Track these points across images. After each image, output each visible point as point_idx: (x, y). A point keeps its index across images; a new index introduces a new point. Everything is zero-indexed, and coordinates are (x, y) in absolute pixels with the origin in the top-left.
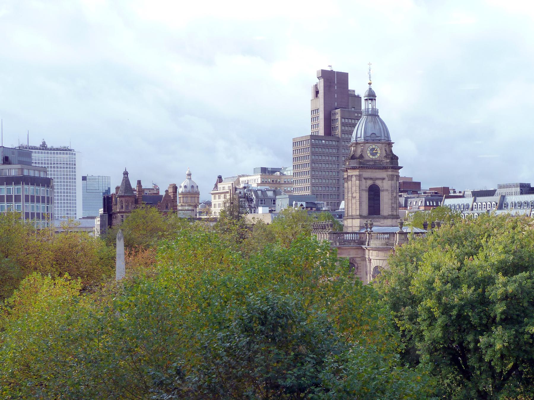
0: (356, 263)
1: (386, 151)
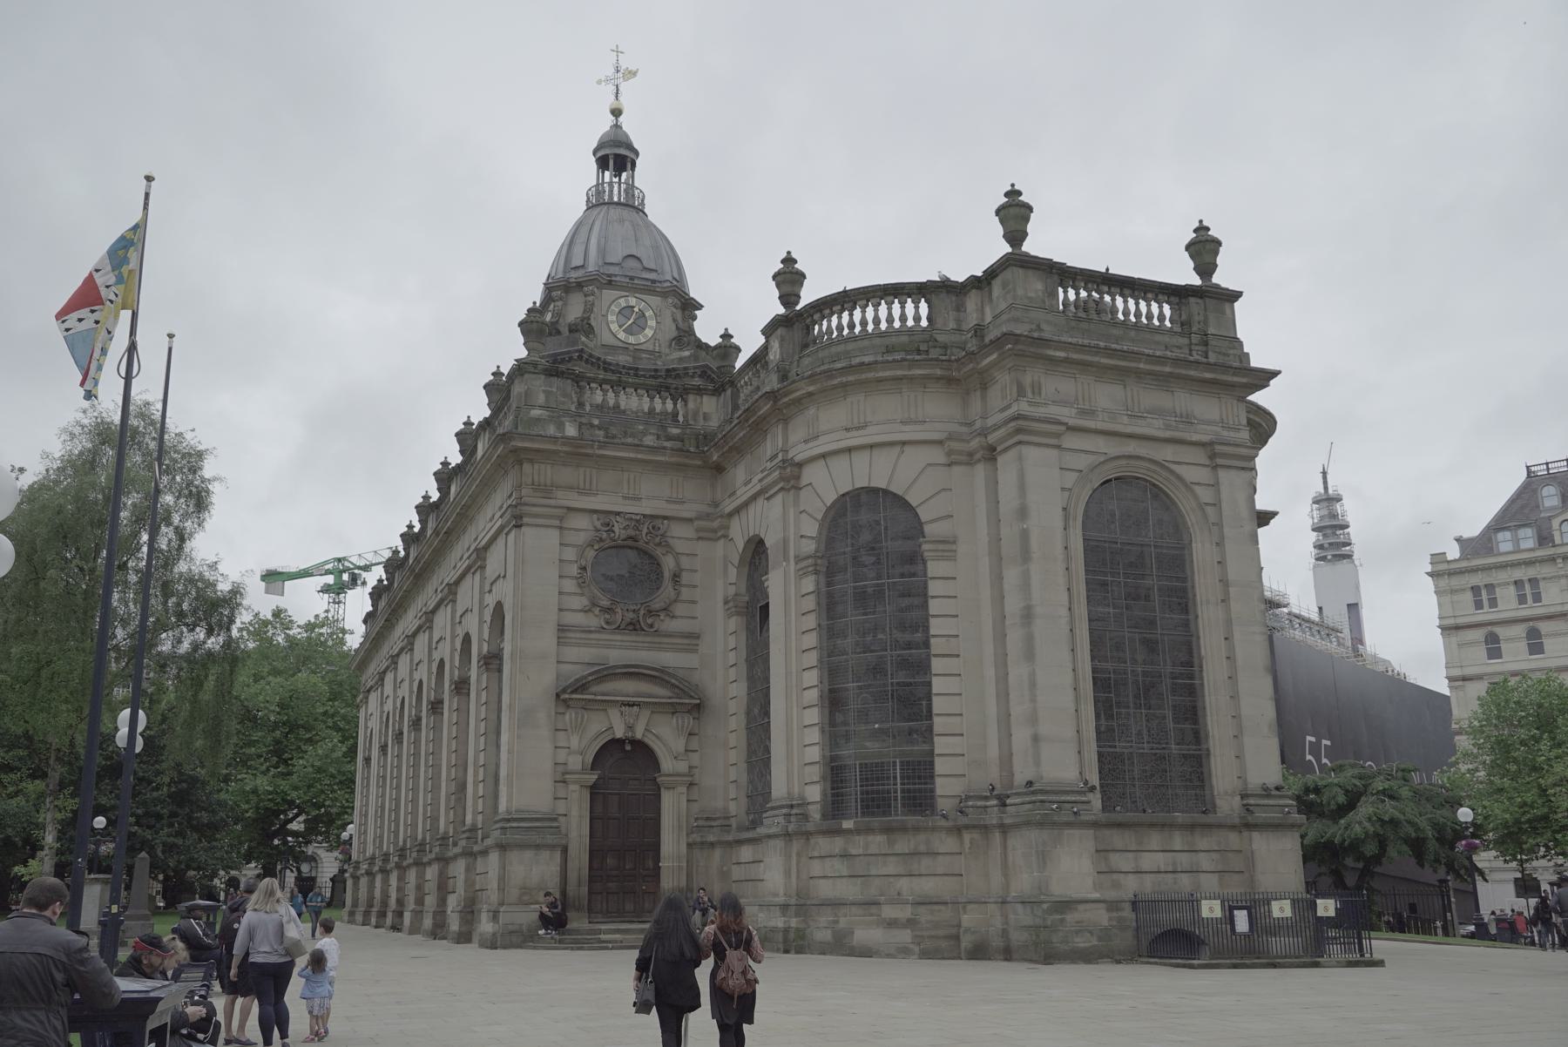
0: (669, 549)
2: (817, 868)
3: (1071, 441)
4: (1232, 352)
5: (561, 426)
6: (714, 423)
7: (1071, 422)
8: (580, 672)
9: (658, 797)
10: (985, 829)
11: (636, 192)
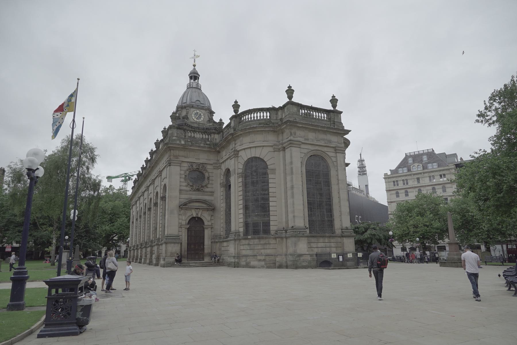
1: (208, 116)
2: (242, 247)
3: (303, 146)
4: (340, 126)
5: (180, 141)
6: (218, 141)
7: (303, 142)
8: (185, 201)
9: (204, 231)
10: (282, 238)
11: (199, 85)
